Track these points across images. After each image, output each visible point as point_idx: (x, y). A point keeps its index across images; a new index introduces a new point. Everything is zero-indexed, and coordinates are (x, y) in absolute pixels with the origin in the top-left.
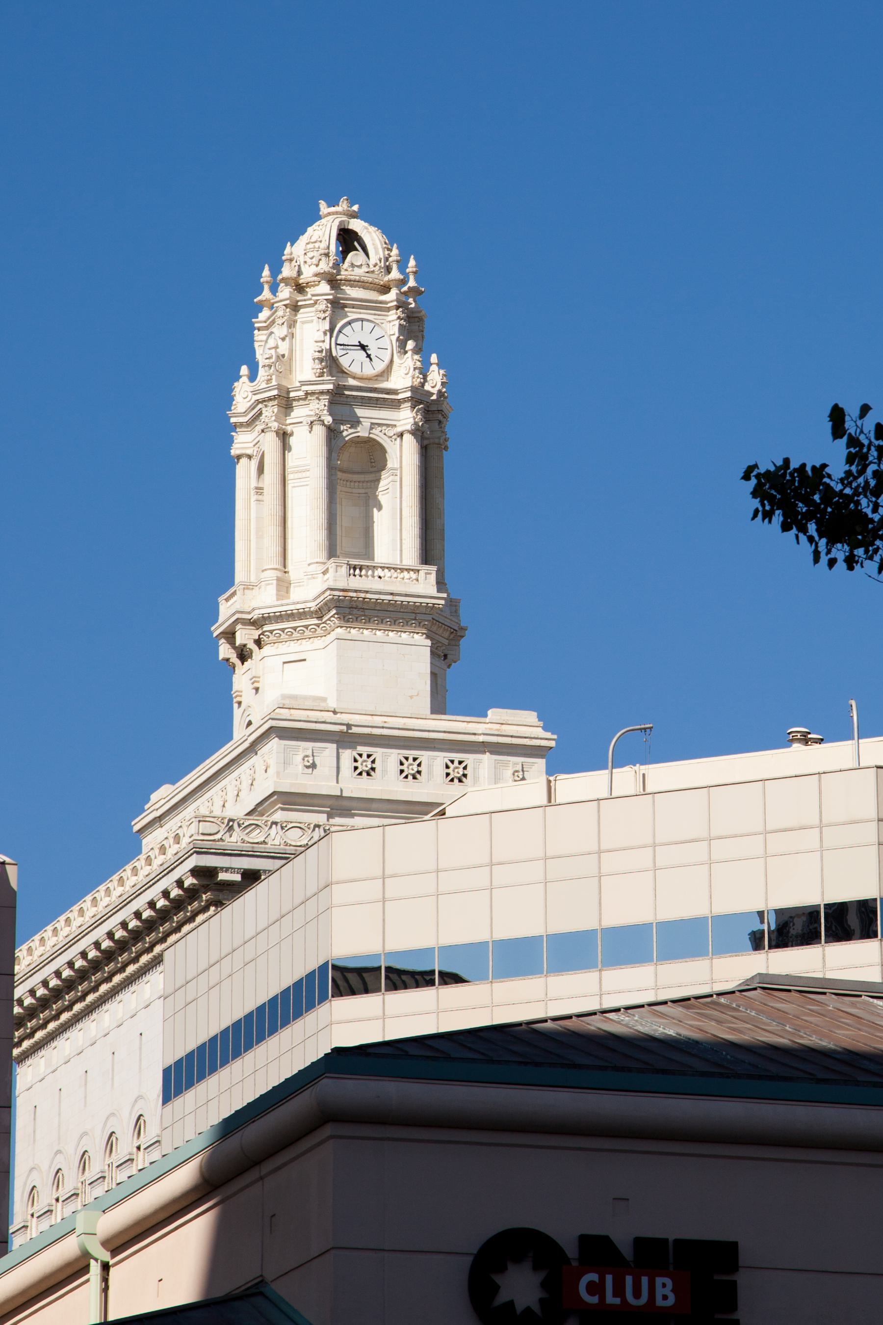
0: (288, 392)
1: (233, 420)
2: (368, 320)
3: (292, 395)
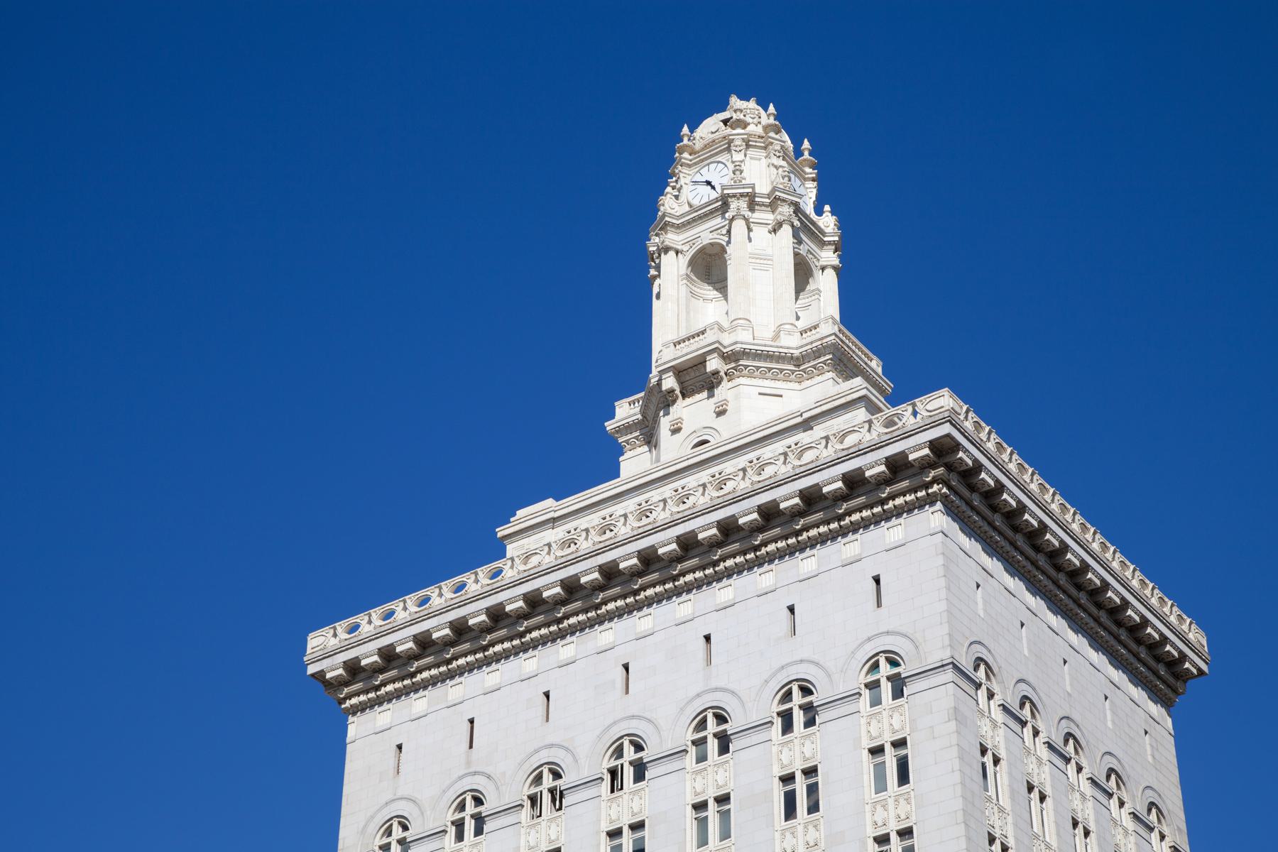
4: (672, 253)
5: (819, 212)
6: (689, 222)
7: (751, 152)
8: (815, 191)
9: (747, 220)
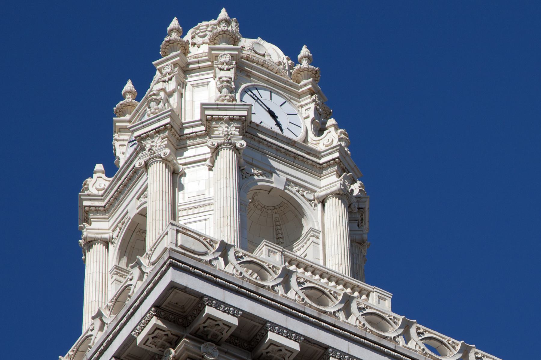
0: (182, 129)
1: (85, 203)
2: (278, 93)
3: (186, 131)
4: (98, 248)
5: (320, 131)
6: (115, 198)
7: (191, 79)
8: (313, 106)
9: (165, 161)
